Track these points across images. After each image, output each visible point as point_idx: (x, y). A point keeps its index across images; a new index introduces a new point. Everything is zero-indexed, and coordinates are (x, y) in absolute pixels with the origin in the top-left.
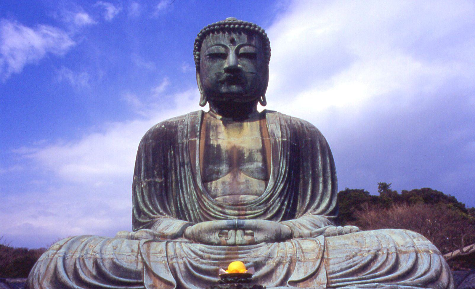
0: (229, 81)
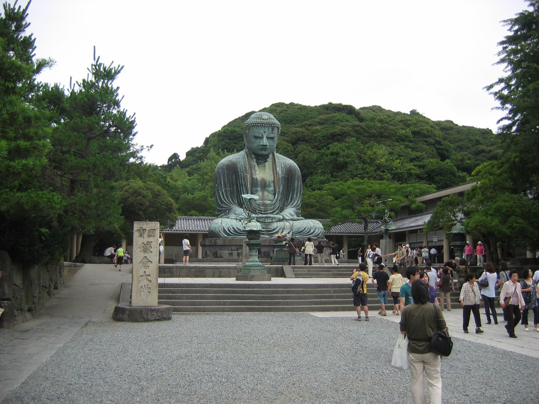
0: (262, 150)
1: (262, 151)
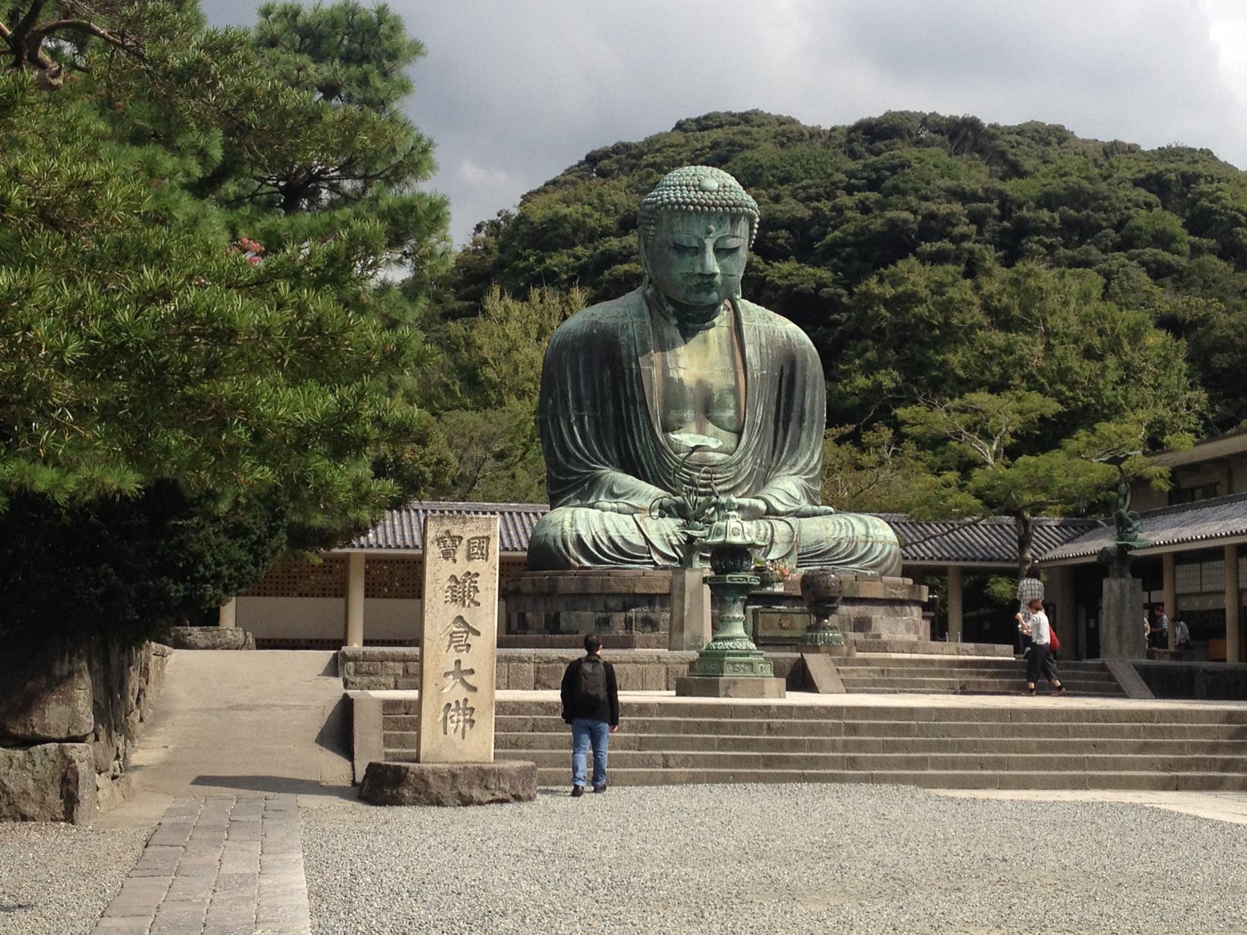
1: (698, 292)
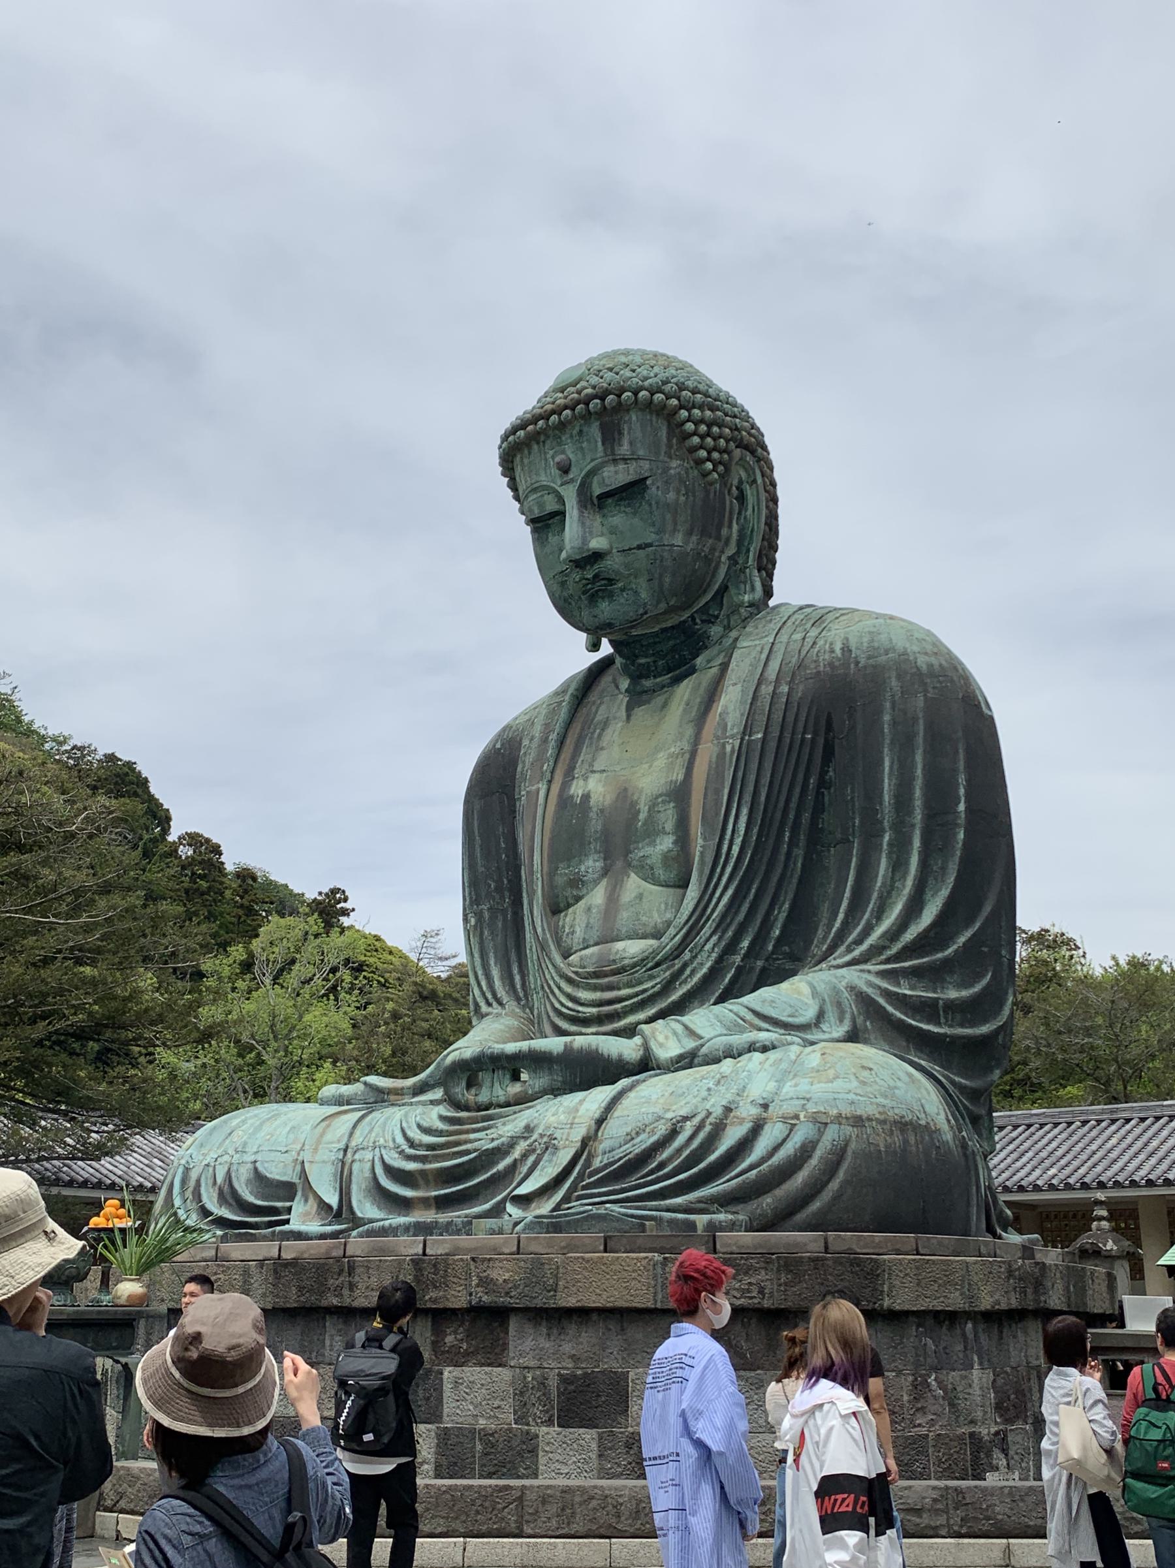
1: (593, 598)
